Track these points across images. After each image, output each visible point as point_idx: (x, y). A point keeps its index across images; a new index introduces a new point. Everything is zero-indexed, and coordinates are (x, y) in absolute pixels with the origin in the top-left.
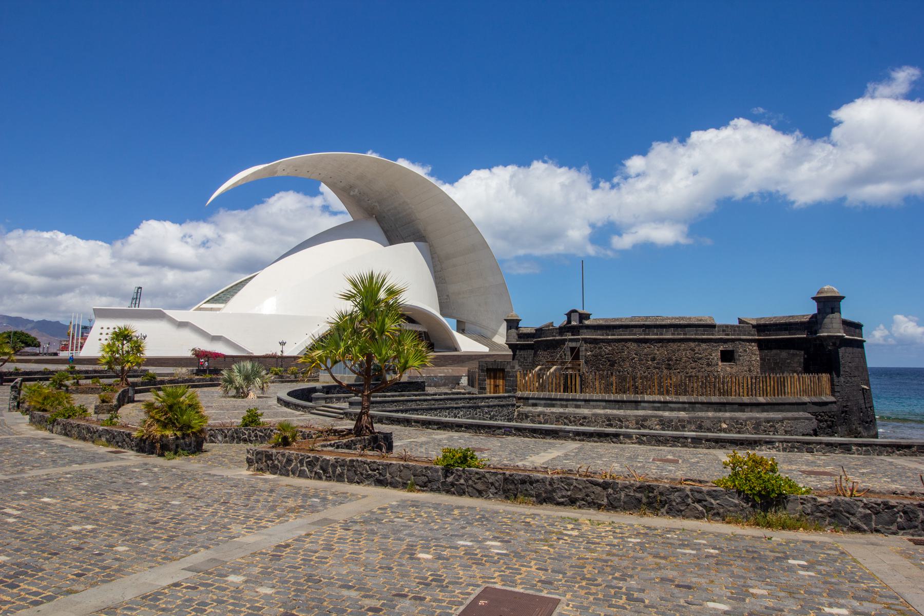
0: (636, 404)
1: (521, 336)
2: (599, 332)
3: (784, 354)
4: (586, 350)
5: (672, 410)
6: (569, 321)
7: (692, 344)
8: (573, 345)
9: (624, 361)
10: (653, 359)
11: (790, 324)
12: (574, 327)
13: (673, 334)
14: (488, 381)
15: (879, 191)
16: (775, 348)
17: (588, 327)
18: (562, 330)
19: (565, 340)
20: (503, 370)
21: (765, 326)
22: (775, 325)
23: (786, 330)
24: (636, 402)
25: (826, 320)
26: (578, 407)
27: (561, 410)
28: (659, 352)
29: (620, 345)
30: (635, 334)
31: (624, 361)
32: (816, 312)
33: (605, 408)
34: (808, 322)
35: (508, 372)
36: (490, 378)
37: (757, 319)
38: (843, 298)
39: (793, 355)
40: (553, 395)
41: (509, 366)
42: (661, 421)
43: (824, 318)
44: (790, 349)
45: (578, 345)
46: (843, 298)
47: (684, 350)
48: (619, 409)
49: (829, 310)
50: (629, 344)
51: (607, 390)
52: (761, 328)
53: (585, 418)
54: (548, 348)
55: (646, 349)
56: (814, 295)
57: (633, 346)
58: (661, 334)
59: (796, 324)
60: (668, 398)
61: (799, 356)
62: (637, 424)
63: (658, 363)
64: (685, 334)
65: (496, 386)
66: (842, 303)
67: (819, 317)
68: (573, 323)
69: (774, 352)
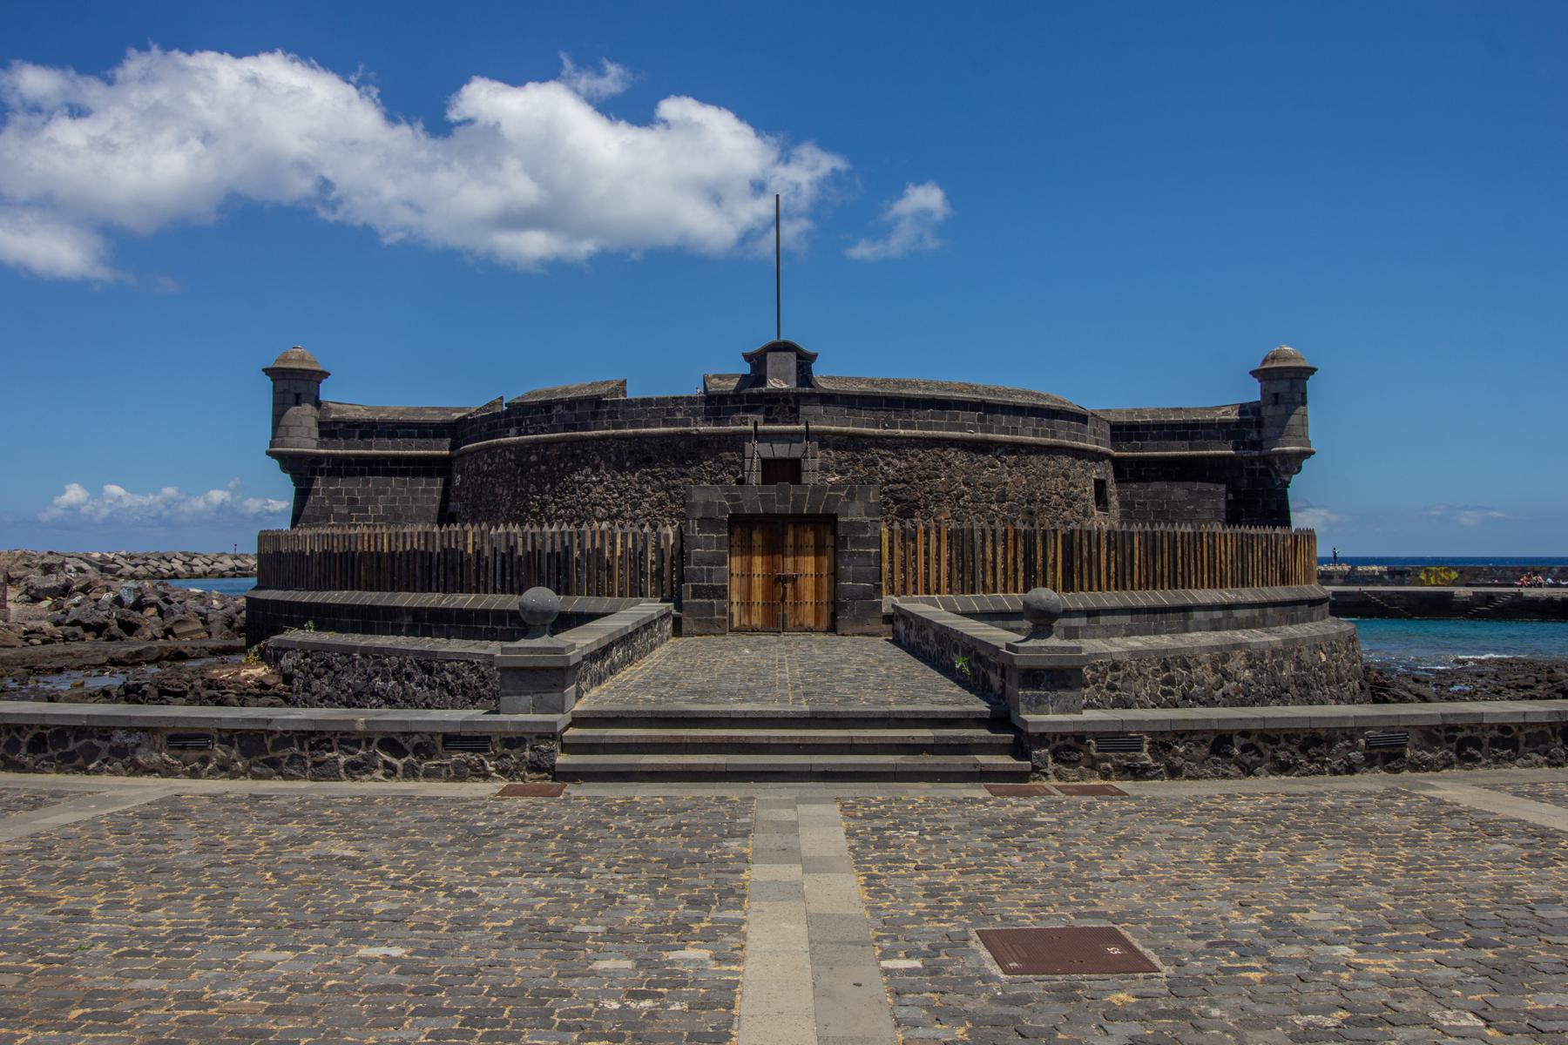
1: (330, 430)
2: (865, 415)
3: (1179, 491)
4: (825, 469)
5: (1239, 625)
6: (758, 375)
7: (1066, 461)
8: (781, 451)
9: (938, 501)
11: (1195, 425)
12: (776, 398)
13: (1035, 433)
14: (736, 563)
15: (534, 244)
16: (1158, 479)
17: (828, 399)
18: (716, 404)
19: (747, 434)
20: (830, 520)
21: (1133, 427)
22: (1159, 426)
23: (1183, 437)
24: (1186, 609)
25: (1294, 419)
26: (1071, 633)
28: (1010, 476)
29: (929, 457)
30: (961, 428)
31: (938, 501)
33: (1130, 632)
34: (1238, 424)
35: (864, 527)
36: (747, 550)
37: (1130, 413)
38: (1312, 370)
39: (1200, 492)
41: (858, 505)
42: (1249, 656)
43: (1289, 414)
44: (1194, 480)
45: (795, 451)
46: (1312, 370)
47: (1054, 475)
48: (1157, 632)
50: (950, 454)
51: (1121, 581)
52: (1123, 432)
53: (1115, 667)
54: (648, 461)
55: (993, 471)
56: (1257, 366)
57: (959, 459)
58: (1015, 431)
59: (1210, 425)
60: (1228, 595)
61: (1216, 495)
62: (1215, 671)
63: (1010, 509)
64: (1054, 435)
65: (777, 582)
66: (1311, 383)
67: (1268, 412)
68: (774, 384)
69: (1156, 486)
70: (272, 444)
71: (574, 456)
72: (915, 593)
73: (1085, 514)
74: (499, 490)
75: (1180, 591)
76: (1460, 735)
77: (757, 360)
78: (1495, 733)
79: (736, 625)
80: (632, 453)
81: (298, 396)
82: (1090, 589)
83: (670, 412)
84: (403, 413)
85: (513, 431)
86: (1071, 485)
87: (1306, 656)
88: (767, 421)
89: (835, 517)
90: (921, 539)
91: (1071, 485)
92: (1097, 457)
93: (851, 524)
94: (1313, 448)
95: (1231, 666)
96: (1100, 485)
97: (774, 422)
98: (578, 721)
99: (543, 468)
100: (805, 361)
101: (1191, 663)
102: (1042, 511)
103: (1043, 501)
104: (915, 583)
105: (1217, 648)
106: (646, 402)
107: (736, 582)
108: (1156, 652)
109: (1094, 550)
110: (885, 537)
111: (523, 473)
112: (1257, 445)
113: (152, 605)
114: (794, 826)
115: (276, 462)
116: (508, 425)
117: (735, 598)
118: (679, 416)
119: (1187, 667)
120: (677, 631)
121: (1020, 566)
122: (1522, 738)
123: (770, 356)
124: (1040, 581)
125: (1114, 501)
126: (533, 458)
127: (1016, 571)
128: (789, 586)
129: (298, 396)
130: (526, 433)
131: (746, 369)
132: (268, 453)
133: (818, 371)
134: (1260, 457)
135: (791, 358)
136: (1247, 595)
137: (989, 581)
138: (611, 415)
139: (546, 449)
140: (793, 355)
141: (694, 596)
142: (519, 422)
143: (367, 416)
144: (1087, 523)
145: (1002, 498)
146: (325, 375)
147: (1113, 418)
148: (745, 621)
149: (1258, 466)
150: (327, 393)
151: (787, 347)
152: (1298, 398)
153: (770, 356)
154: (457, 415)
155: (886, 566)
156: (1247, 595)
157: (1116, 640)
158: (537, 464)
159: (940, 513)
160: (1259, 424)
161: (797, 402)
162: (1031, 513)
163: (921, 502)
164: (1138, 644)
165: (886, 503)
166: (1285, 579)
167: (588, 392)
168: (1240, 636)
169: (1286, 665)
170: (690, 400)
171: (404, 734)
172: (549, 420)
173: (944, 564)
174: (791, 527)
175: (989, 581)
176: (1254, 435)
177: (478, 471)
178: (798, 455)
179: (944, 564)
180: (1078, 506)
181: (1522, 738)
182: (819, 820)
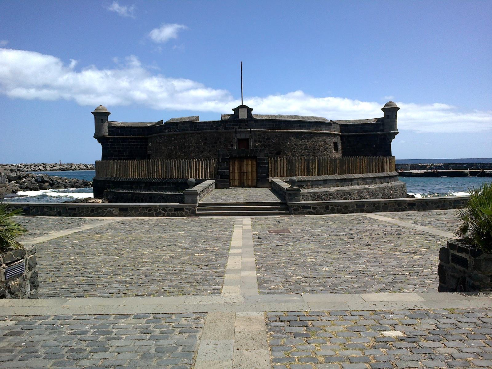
0: (350, 181)
5: (367, 183)
8: (243, 136)
10: (306, 149)
27: (311, 190)
32: (383, 116)
40: (301, 178)
42: (368, 192)
47: (321, 141)
49: (394, 117)
51: (333, 173)
62: (359, 196)
63: (308, 152)
68: (240, 117)
71: (184, 138)
72: (278, 176)
73: (330, 152)
74: (163, 148)
75: (350, 175)
76: (376, 205)
77: (236, 110)
78: (383, 205)
79: (231, 185)
80: (201, 137)
81: (102, 120)
82: (325, 175)
83: (212, 126)
84: (133, 124)
85: (167, 131)
86: (326, 144)
87: (386, 191)
88: (239, 128)
89: (257, 157)
90: (279, 162)
91: (326, 144)
92: (335, 135)
93: (261, 159)
94: (398, 131)
95: (363, 195)
96: (336, 144)
97: (241, 128)
98: (200, 205)
99: (176, 142)
100: (250, 110)
101: (352, 194)
102: (318, 152)
103: (318, 149)
104: (277, 174)
105: (359, 190)
106: (205, 122)
107: (231, 173)
108: (342, 191)
109: (326, 164)
110: (270, 162)
111: (170, 143)
112: (382, 131)
113: (47, 182)
114: (242, 221)
115: (96, 140)
116: (165, 129)
117: (231, 178)
118: (214, 127)
119: (351, 195)
120: (216, 188)
121: (306, 169)
122: (389, 206)
123: (240, 110)
124: (311, 173)
125: (340, 148)
127: (304, 170)
128: (245, 174)
129: (102, 120)
131: (233, 113)
132: (94, 137)
133: (253, 113)
134: (383, 134)
135: (246, 110)
136: (371, 175)
137: (297, 173)
138: (195, 126)
139: (177, 136)
140: (246, 110)
141: (220, 178)
142: (169, 128)
143: (122, 125)
144: (331, 155)
145: (306, 149)
146: (109, 113)
147: (341, 123)
148: (234, 184)
149: (383, 137)
150: (110, 118)
151: (245, 107)
152: (394, 117)
153: (240, 110)
154: (149, 125)
155: (270, 169)
156: (371, 175)
157: (332, 188)
158: (174, 140)
159: (288, 154)
160: (383, 124)
161: (247, 122)
162: (314, 153)
163: (282, 151)
164: (337, 189)
165: (273, 150)
166: (383, 170)
167: (188, 120)
168: (367, 186)
169: (380, 194)
170: (217, 122)
171: (167, 207)
172: (178, 127)
173: (285, 169)
174: (245, 160)
175: (297, 173)
176: (381, 128)
177: (157, 142)
178: (248, 138)
179: (285, 169)
180: (328, 150)
181: (389, 206)
182: (247, 220)
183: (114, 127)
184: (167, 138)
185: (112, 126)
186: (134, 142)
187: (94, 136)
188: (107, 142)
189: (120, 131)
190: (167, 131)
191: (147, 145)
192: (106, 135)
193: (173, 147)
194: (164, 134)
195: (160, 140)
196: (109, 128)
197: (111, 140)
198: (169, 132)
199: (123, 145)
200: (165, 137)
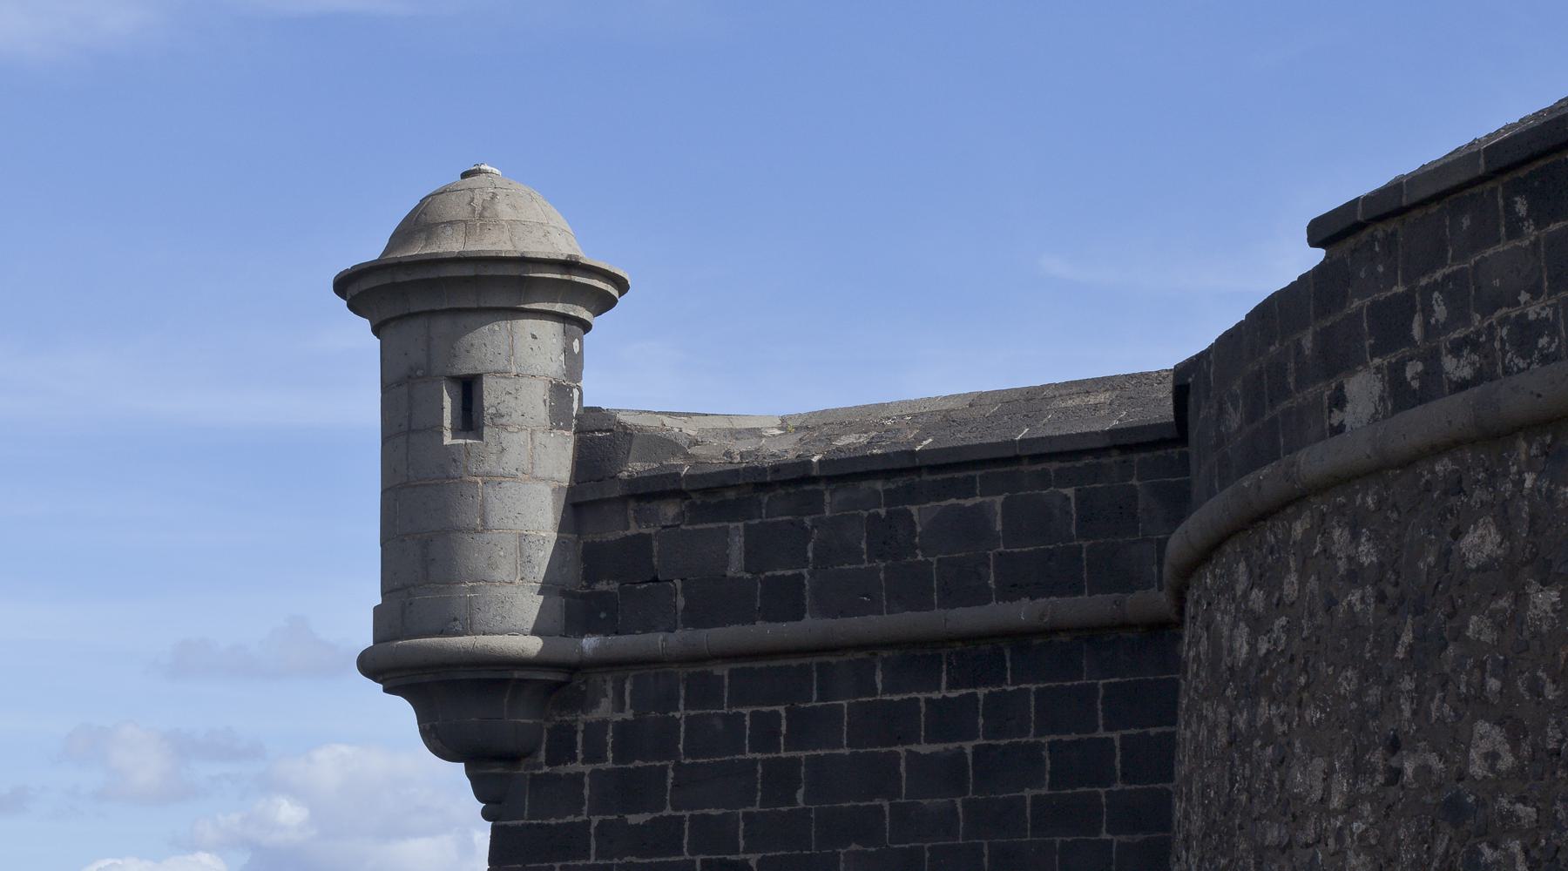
70: (388, 621)
74: (1306, 779)
85: (1363, 389)
99: (1544, 600)
115: (401, 713)
116: (1336, 360)
126: (1481, 542)
130: (1433, 386)
132: (371, 666)
143: (786, 448)
183: (650, 492)
184: (1367, 554)
185: (635, 467)
186: (948, 720)
187: (366, 639)
188: (562, 748)
189: (735, 567)
190: (1363, 389)
191: (1156, 760)
192: (512, 616)
193: (1487, 735)
194: (1314, 461)
195: (1258, 625)
196: (579, 507)
197: (604, 710)
198: (1400, 396)
199: (781, 778)
200: (1339, 535)
